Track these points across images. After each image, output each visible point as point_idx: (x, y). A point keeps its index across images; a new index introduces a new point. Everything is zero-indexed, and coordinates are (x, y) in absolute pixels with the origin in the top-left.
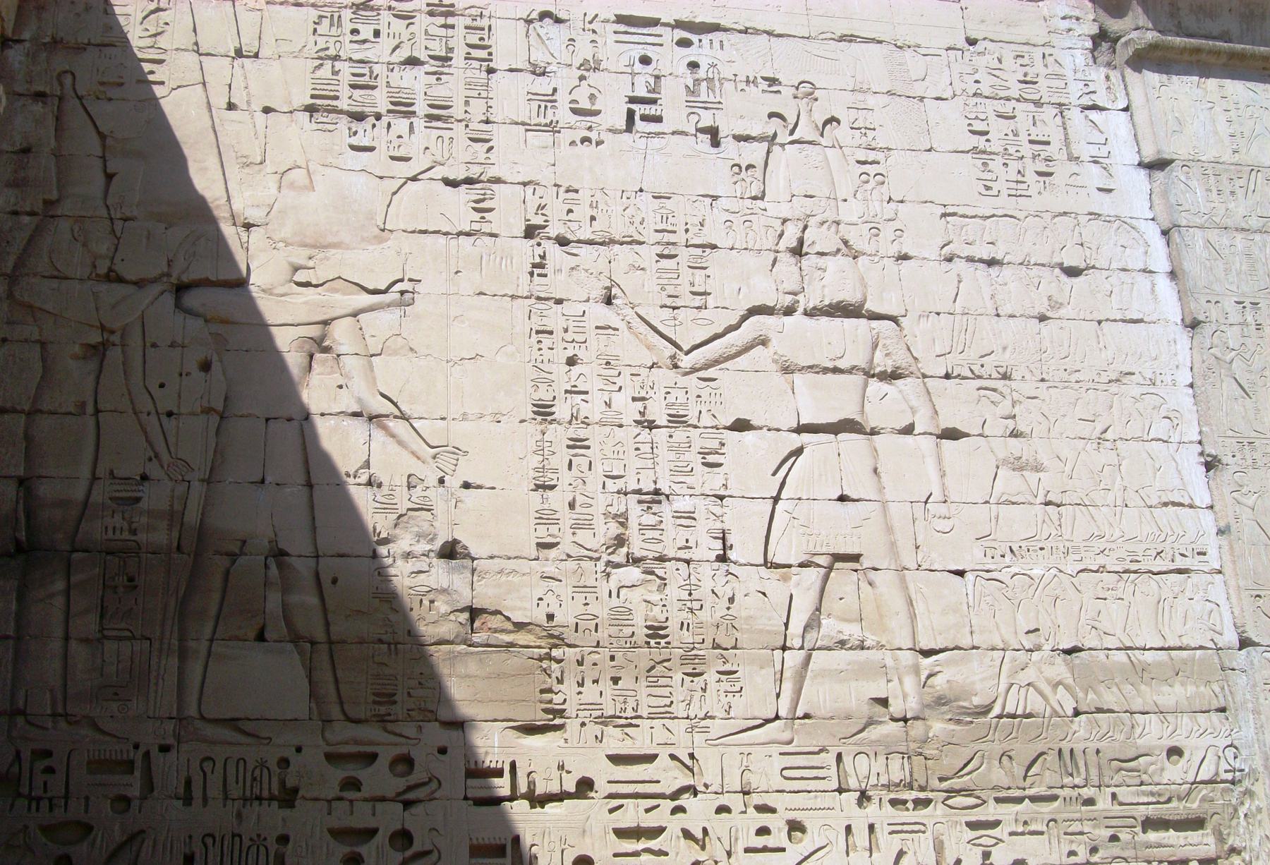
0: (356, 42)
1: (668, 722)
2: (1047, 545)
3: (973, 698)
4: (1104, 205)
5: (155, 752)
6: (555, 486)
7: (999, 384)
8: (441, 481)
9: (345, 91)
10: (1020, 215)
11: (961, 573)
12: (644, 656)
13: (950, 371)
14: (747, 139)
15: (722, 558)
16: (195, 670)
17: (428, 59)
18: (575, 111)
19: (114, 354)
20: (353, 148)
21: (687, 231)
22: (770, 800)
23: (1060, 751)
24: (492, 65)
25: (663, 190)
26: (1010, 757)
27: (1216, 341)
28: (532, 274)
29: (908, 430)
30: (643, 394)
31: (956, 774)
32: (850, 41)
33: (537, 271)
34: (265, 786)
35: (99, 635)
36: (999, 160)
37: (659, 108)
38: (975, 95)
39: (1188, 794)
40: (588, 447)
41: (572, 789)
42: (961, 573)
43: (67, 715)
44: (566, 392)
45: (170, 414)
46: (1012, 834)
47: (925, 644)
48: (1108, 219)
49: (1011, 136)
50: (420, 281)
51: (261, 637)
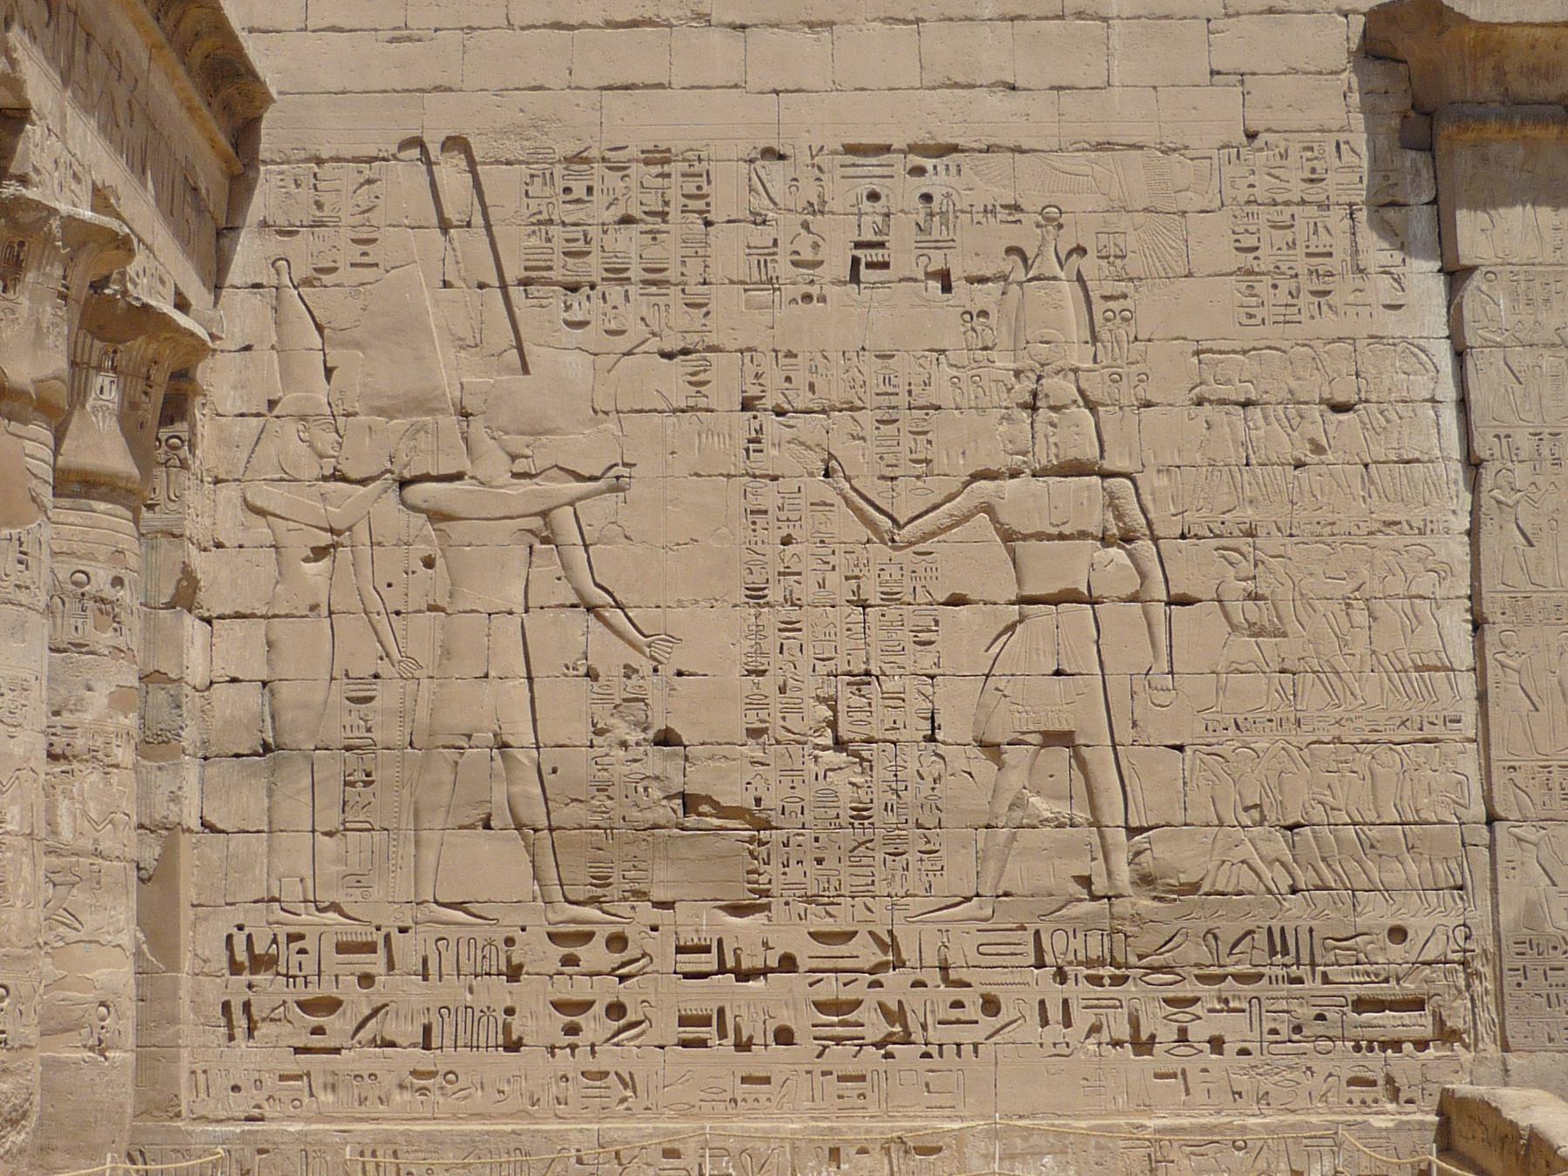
0: (569, 202)
1: (869, 901)
2: (1276, 716)
3: (1181, 875)
4: (1391, 324)
5: (395, 934)
6: (765, 671)
7: (1243, 543)
8: (656, 670)
9: (558, 260)
10: (1285, 345)
11: (1180, 748)
12: (847, 837)
13: (1186, 531)
14: (982, 280)
15: (931, 739)
16: (429, 856)
17: (644, 216)
18: (795, 264)
19: (344, 553)
20: (569, 324)
21: (910, 392)
22: (964, 975)
23: (1270, 930)
24: (710, 217)
25: (887, 346)
26: (1216, 938)
27: (1501, 481)
28: (747, 450)
29: (1134, 598)
30: (856, 572)
31: (1155, 952)
32: (1107, 150)
33: (751, 446)
34: (494, 963)
35: (342, 828)
36: (1268, 280)
37: (885, 252)
38: (1248, 202)
39: (1407, 974)
40: (800, 630)
41: (776, 965)
42: (1180, 748)
43: (315, 902)
44: (780, 574)
45: (398, 613)
46: (1210, 1011)
47: (1134, 823)
48: (1391, 341)
49: (1285, 251)
50: (634, 465)
51: (487, 826)
